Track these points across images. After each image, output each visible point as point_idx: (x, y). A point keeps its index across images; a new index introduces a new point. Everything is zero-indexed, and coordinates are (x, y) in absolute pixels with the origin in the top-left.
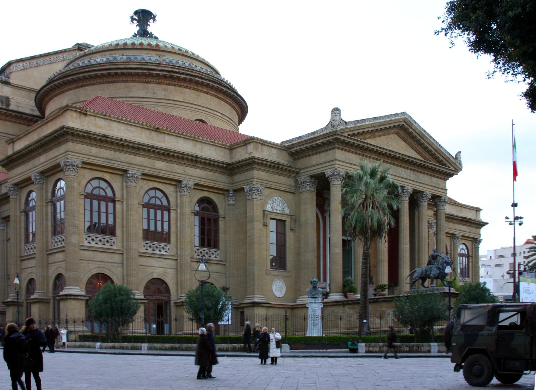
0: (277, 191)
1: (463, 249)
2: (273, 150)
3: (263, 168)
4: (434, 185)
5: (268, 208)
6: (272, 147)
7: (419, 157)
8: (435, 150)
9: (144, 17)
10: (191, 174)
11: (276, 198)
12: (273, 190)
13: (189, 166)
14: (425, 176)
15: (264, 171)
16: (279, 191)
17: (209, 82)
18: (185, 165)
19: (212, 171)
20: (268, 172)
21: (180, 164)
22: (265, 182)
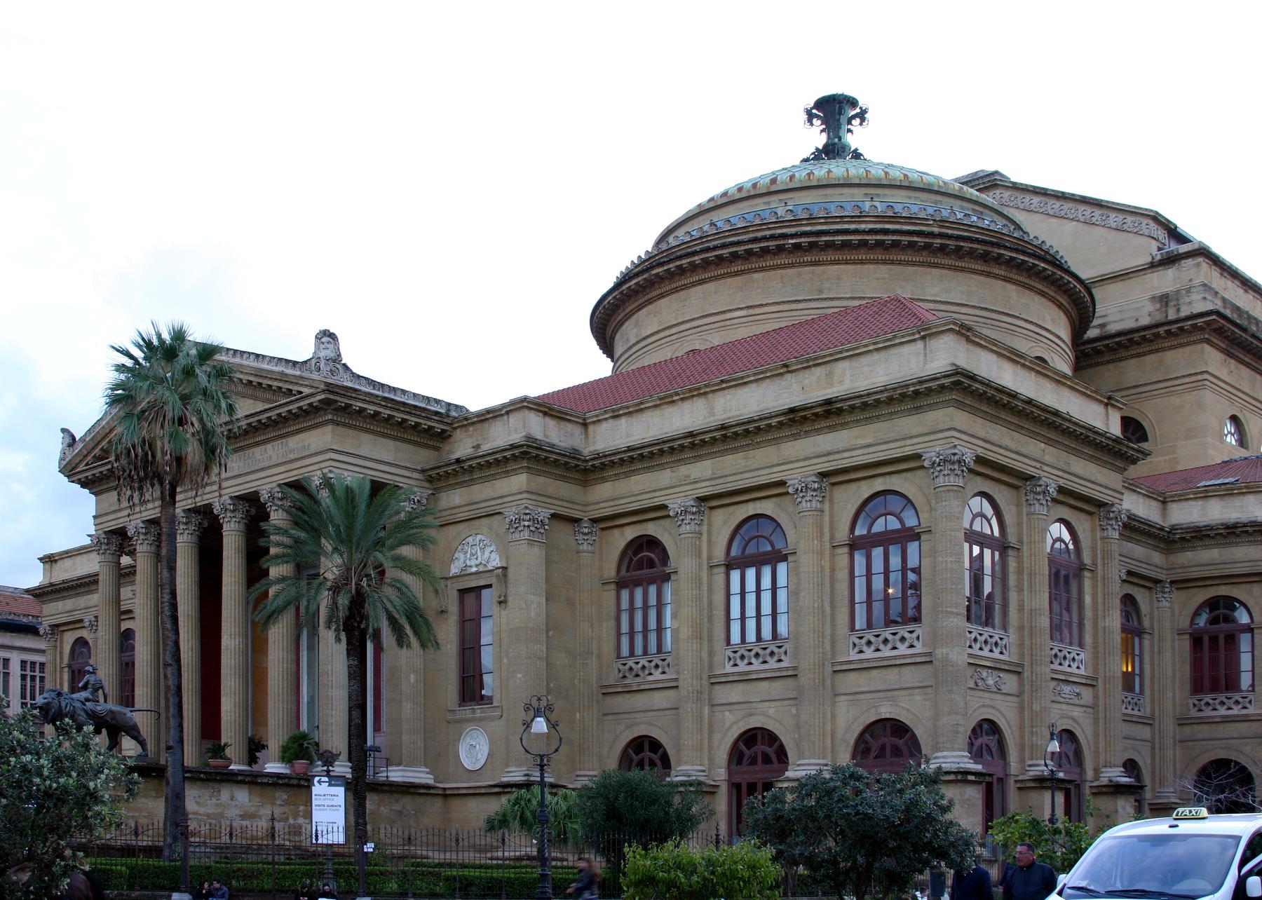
1: (983, 516)
4: (292, 456)
7: (260, 406)
9: (834, 111)
14: (269, 446)
17: (678, 263)
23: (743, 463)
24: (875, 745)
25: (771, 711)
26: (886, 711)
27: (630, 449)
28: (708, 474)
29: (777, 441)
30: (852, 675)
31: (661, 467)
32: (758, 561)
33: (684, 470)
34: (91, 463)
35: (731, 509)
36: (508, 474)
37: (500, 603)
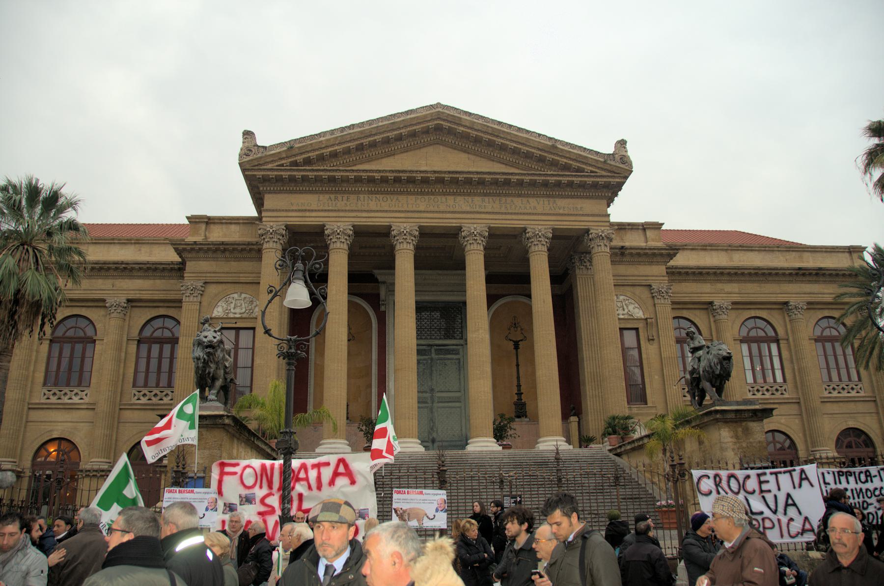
0: (237, 285)
2: (233, 227)
3: (201, 255)
4: (561, 211)
5: (218, 312)
6: (231, 223)
8: (539, 149)
10: (125, 287)
11: (236, 296)
12: (229, 285)
13: (122, 277)
14: (531, 200)
15: (206, 259)
16: (240, 285)
18: (114, 277)
19: (163, 277)
20: (215, 259)
21: (106, 277)
22: (208, 275)
23: (758, 289)
24: (846, 441)
25: (783, 421)
26: (852, 424)
27: (698, 268)
28: (737, 290)
29: (779, 282)
30: (828, 404)
31: (705, 281)
32: (758, 340)
33: (719, 286)
34: (268, 171)
35: (740, 311)
36: (651, 263)
37: (649, 340)
